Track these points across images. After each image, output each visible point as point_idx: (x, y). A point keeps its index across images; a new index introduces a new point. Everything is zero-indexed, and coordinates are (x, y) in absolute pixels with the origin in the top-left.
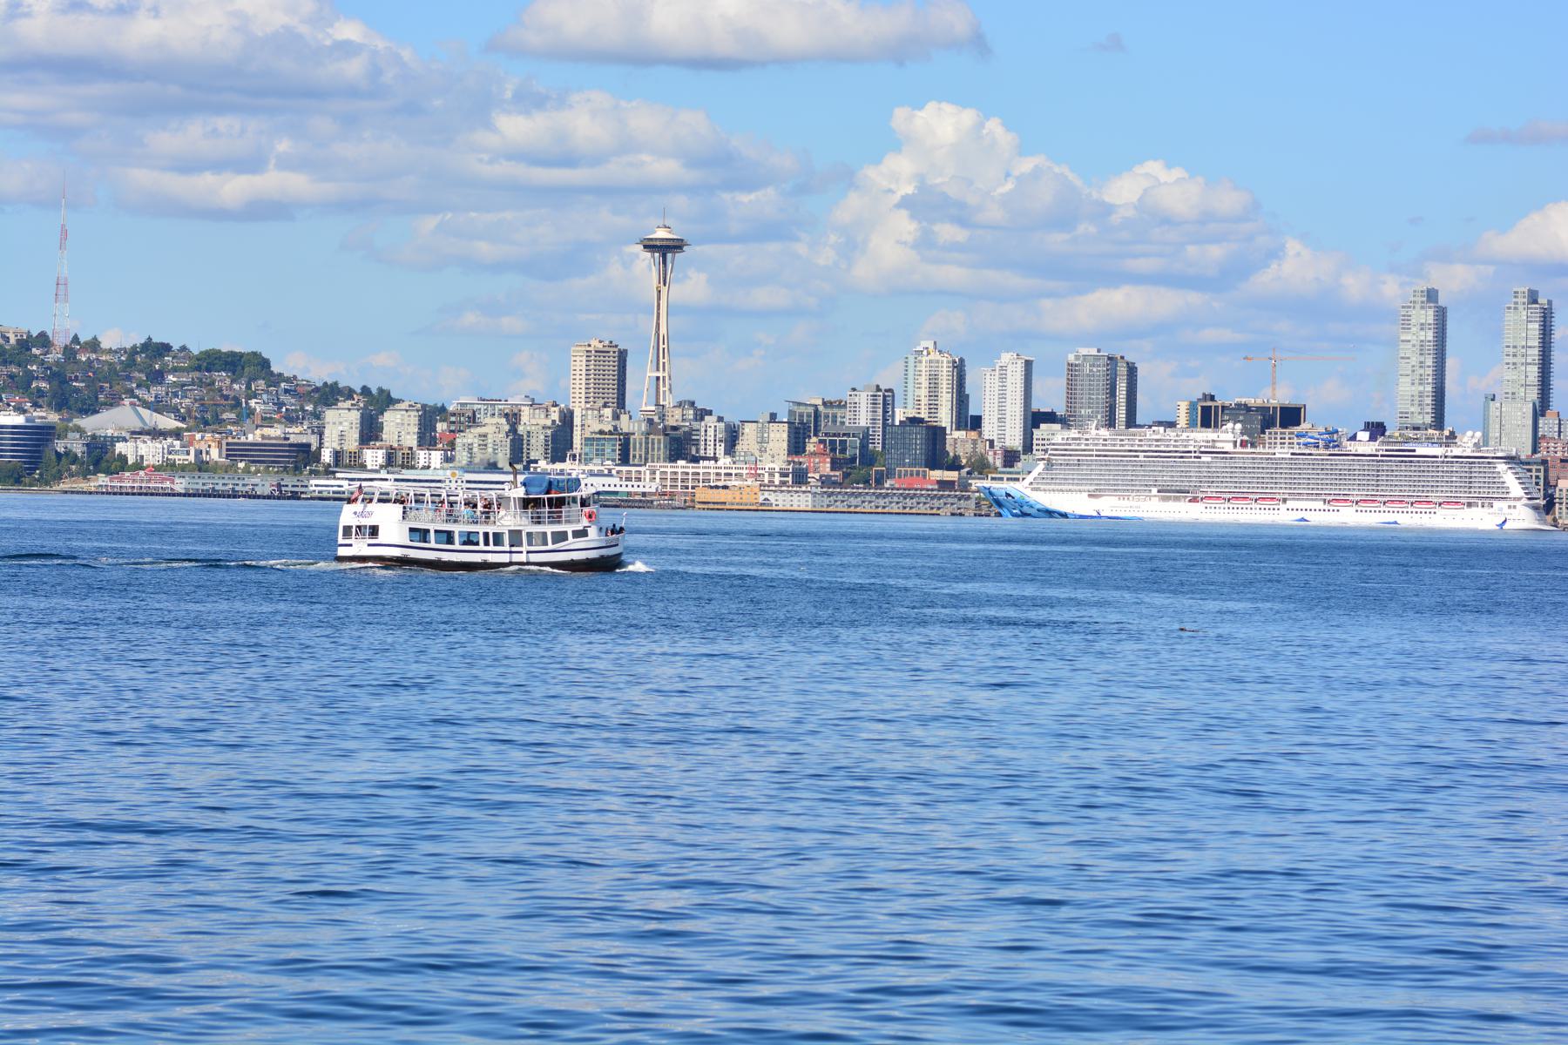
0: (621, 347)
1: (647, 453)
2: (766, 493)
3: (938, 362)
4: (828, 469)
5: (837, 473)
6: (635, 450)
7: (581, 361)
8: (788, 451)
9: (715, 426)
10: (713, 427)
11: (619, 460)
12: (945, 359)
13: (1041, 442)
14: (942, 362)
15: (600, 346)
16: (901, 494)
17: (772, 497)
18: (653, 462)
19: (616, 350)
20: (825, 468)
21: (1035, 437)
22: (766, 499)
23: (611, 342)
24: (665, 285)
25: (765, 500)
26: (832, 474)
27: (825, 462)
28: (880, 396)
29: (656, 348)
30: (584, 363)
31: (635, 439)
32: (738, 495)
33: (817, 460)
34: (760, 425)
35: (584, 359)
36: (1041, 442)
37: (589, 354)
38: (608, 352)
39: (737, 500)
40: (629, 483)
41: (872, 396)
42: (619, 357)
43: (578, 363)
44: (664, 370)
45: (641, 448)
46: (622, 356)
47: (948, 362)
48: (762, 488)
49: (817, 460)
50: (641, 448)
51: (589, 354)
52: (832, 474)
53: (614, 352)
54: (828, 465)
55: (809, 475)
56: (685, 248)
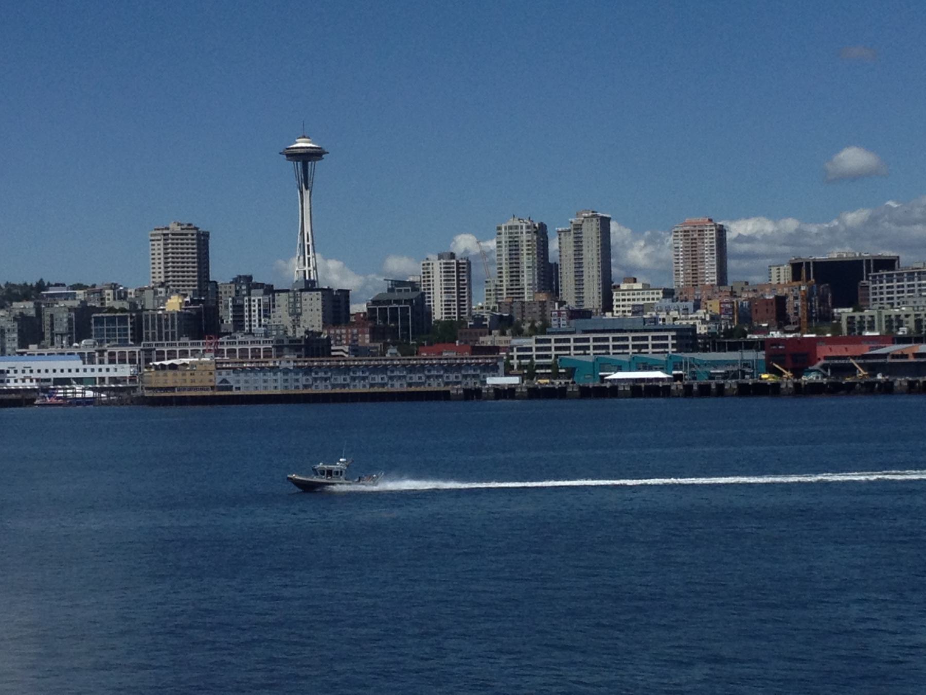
0: (202, 229)
1: (160, 332)
2: (224, 372)
3: (517, 227)
4: (367, 341)
5: (378, 345)
6: (147, 328)
7: (159, 245)
8: (324, 322)
9: (259, 300)
10: (257, 301)
11: (131, 340)
12: (524, 225)
13: (621, 303)
14: (522, 227)
15: (178, 229)
16: (366, 366)
17: (232, 378)
18: (147, 339)
19: (194, 232)
20: (364, 339)
21: (615, 297)
22: (224, 381)
23: (189, 225)
24: (307, 188)
25: (221, 382)
26: (373, 345)
27: (364, 333)
28: (453, 263)
29: (302, 246)
30: (162, 247)
31: (147, 316)
32: (188, 377)
33: (355, 331)
34: (291, 294)
35: (161, 242)
36: (621, 303)
37: (166, 237)
38: (186, 234)
39: (188, 384)
40: (104, 367)
41: (444, 264)
42: (198, 239)
43: (156, 247)
44: (309, 265)
45: (153, 326)
46: (203, 240)
47: (528, 227)
48: (219, 366)
49: (355, 331)
50: (153, 326)
51: (166, 237)
52: (373, 345)
53: (193, 235)
54: (367, 336)
55: (333, 348)
56: (323, 156)
